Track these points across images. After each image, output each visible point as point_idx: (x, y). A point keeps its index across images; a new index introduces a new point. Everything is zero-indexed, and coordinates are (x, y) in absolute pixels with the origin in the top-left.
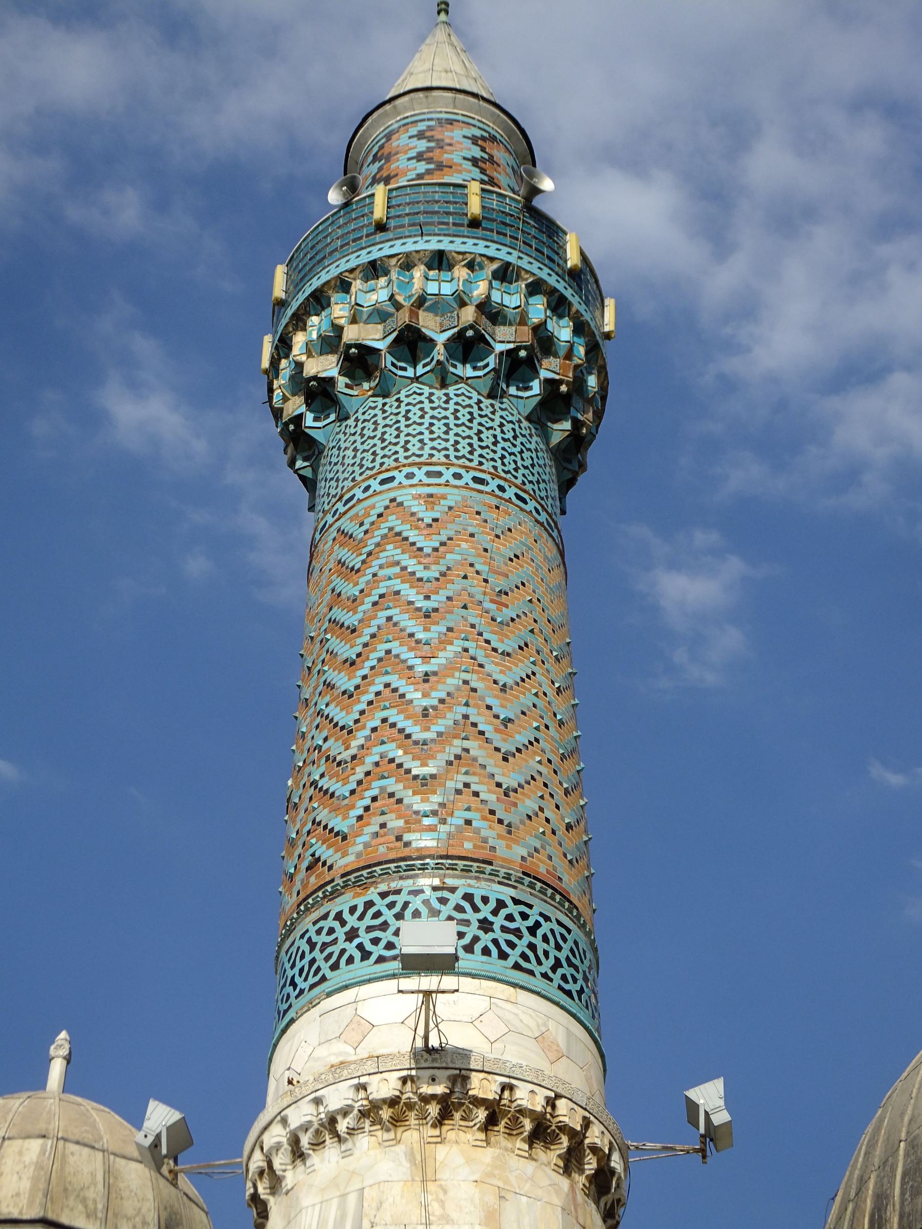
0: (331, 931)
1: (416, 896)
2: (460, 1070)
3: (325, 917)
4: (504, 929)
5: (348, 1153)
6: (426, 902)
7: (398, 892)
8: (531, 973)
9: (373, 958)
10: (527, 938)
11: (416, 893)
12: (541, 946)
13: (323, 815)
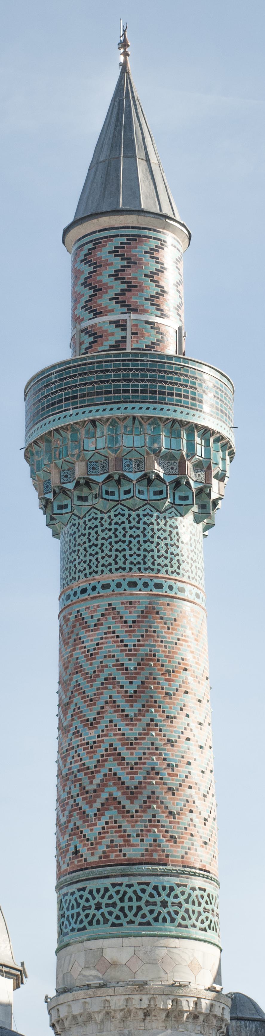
0: (87, 900)
2: (153, 994)
6: (135, 892)
7: (121, 885)
9: (110, 923)
11: (130, 886)
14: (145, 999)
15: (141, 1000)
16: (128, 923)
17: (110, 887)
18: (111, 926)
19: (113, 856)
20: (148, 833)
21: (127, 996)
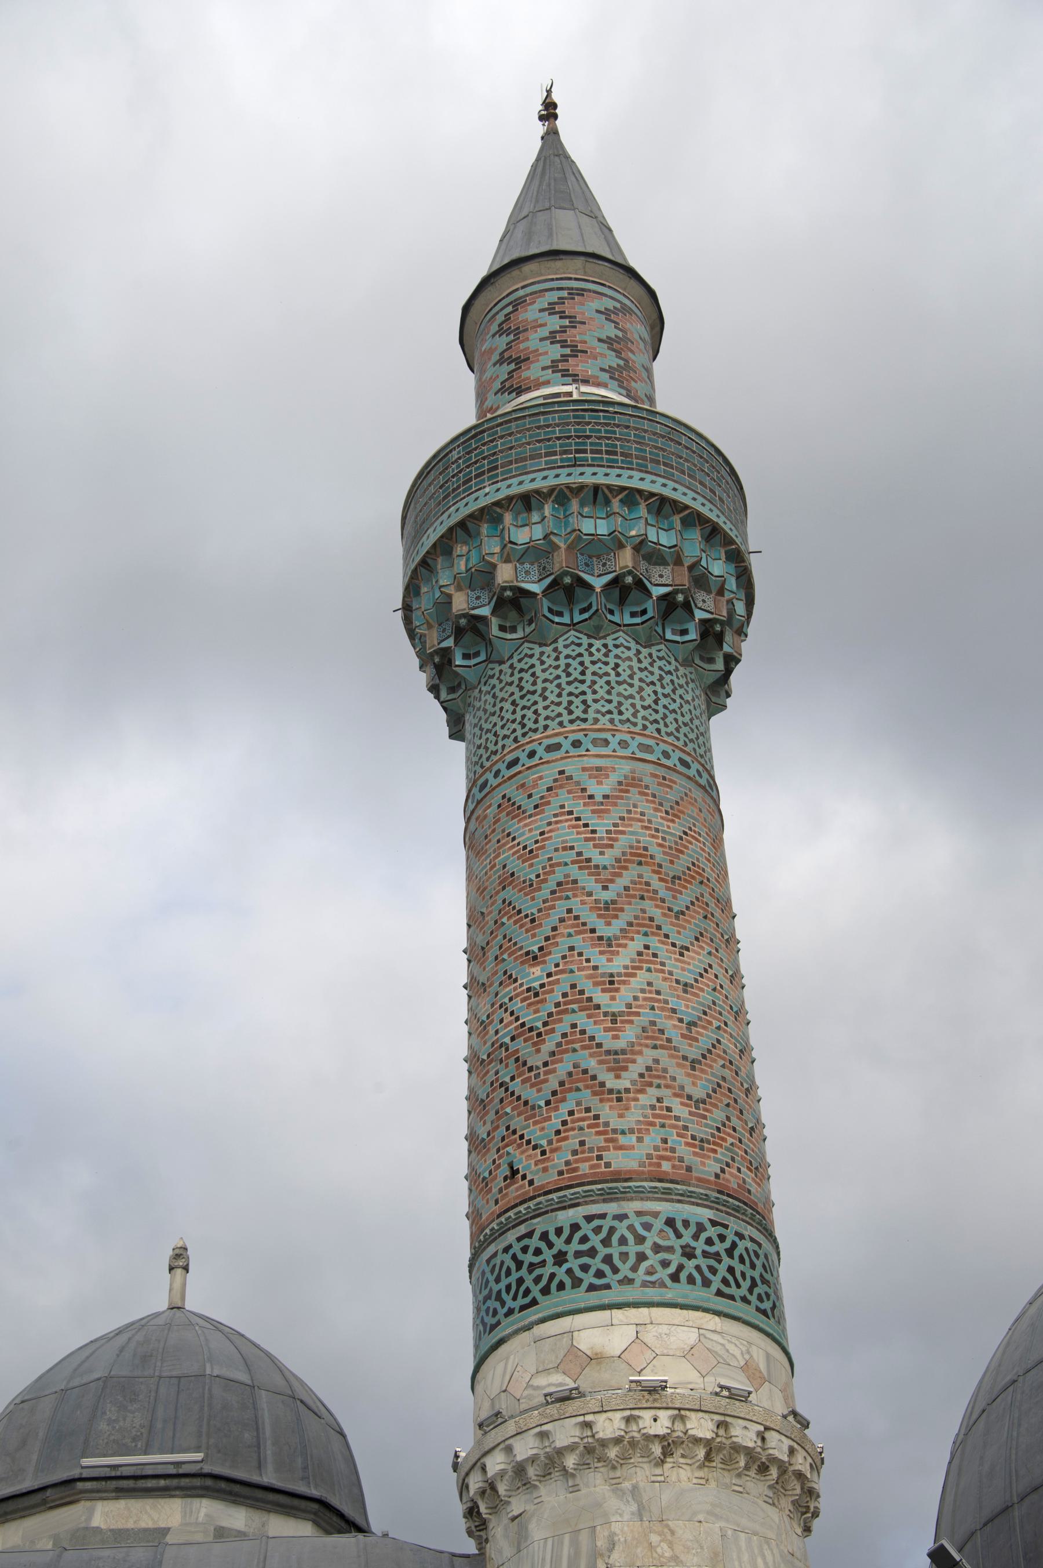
0: (538, 1252)
1: (621, 1222)
2: (679, 1409)
3: (530, 1235)
4: (705, 1254)
5: (576, 1488)
6: (631, 1228)
7: (603, 1216)
8: (732, 1298)
9: (585, 1285)
10: (726, 1261)
11: (621, 1217)
12: (739, 1268)
13: (517, 1122)
14: (664, 1416)
15: (655, 1420)
16: (620, 1282)
17: (583, 1223)
18: (587, 1291)
19: (584, 1168)
20: (651, 1128)
21: (627, 1413)
